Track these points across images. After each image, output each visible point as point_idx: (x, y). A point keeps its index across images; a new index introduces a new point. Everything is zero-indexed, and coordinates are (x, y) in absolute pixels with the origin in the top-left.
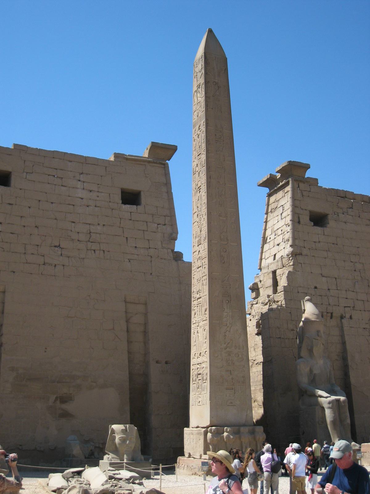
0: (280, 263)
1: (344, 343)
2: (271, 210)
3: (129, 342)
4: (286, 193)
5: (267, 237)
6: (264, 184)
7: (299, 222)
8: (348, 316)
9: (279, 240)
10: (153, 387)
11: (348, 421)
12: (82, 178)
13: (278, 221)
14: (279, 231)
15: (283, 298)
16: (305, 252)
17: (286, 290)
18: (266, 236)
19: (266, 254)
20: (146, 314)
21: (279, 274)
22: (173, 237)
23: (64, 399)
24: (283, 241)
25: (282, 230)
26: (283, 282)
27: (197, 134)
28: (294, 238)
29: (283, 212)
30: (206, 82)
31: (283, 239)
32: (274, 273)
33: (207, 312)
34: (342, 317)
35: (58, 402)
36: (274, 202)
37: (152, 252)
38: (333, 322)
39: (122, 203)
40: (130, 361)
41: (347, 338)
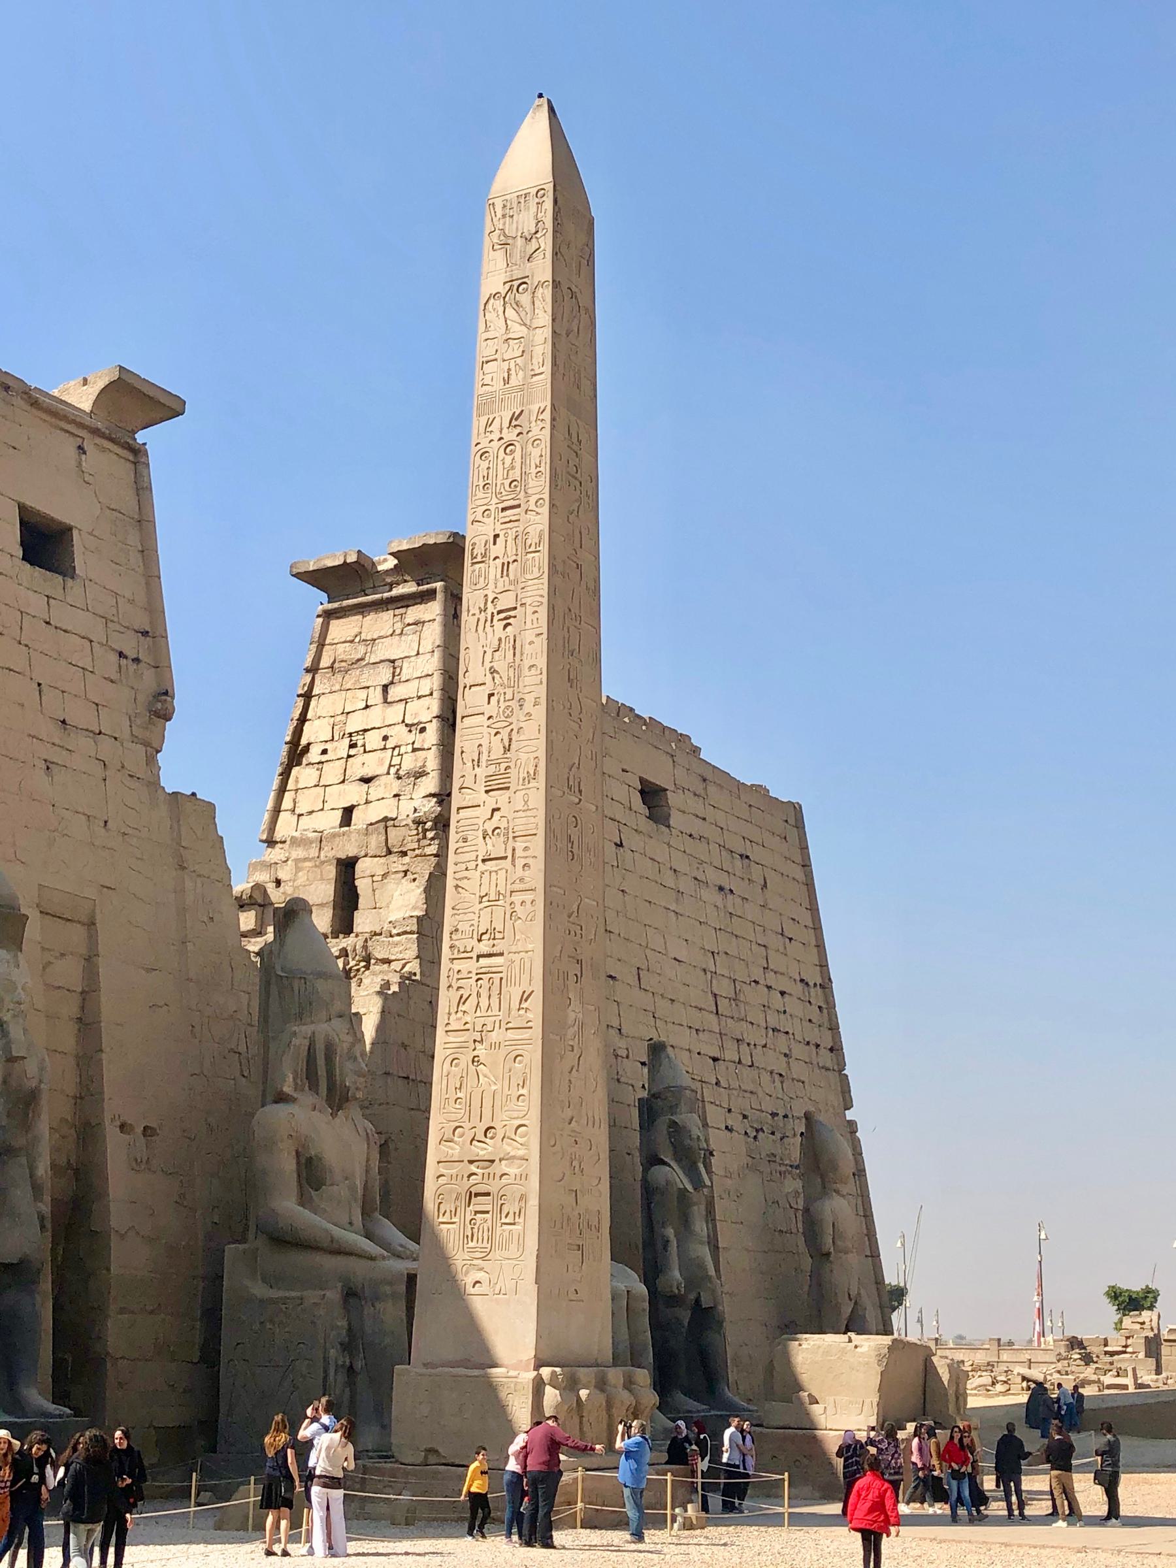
2: (334, 662)
4: (409, 625)
5: (309, 744)
6: (318, 578)
13: (367, 707)
18: (304, 742)
19: (301, 796)
20: (90, 960)
21: (368, 873)
24: (388, 773)
25: (385, 738)
27: (501, 439)
29: (392, 683)
31: (390, 766)
32: (347, 867)
33: (536, 1004)
36: (352, 642)
39: (23, 559)
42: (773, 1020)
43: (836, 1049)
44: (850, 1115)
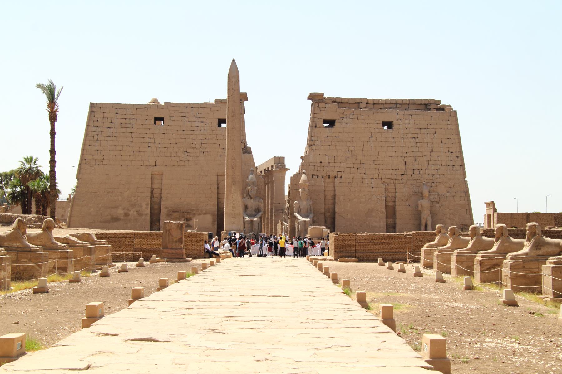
7: (316, 127)
8: (339, 176)
16: (317, 143)
34: (335, 177)
38: (330, 180)
42: (430, 163)
43: (462, 165)
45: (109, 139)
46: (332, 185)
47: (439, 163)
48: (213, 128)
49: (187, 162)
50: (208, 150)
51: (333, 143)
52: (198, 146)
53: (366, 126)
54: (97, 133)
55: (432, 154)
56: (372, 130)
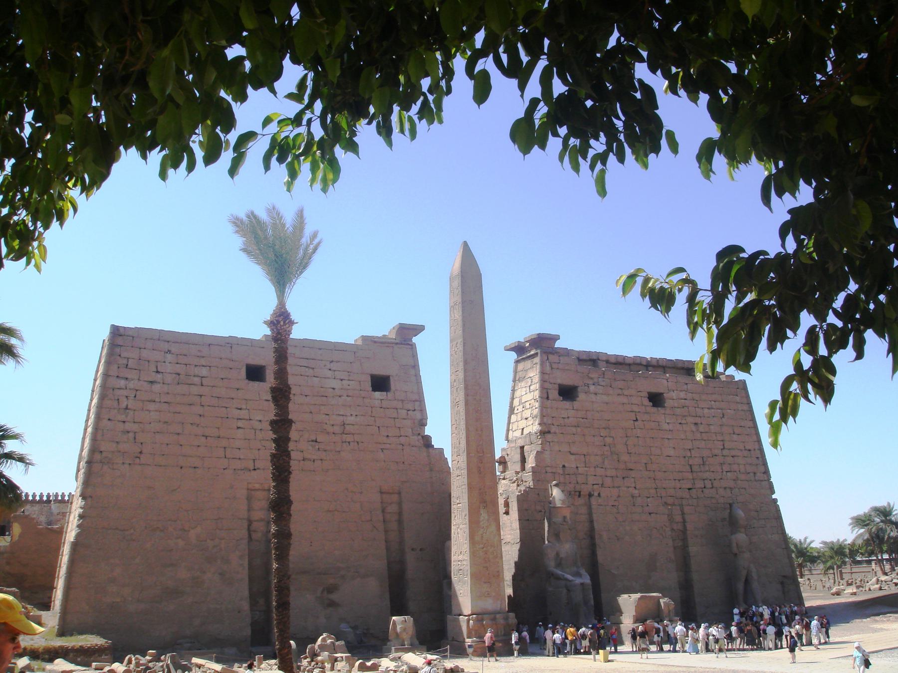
0: (528, 439)
1: (591, 522)
3: (386, 531)
7: (548, 398)
8: (596, 494)
9: (527, 413)
10: (410, 573)
11: (592, 602)
12: (334, 366)
14: (527, 404)
15: (531, 479)
17: (534, 471)
20: (400, 504)
22: (423, 423)
23: (331, 589)
26: (531, 463)
28: (543, 415)
30: (463, 302)
32: (522, 448)
34: (590, 495)
35: (325, 593)
37: (402, 440)
38: (581, 501)
40: (388, 549)
41: (595, 517)
43: (767, 472)
44: (774, 496)
45: (152, 406)
46: (584, 510)
47: (735, 467)
48: (363, 394)
49: (318, 463)
50: (357, 438)
51: (579, 429)
52: (337, 429)
53: (625, 400)
54: (125, 393)
55: (725, 452)
56: (635, 408)
